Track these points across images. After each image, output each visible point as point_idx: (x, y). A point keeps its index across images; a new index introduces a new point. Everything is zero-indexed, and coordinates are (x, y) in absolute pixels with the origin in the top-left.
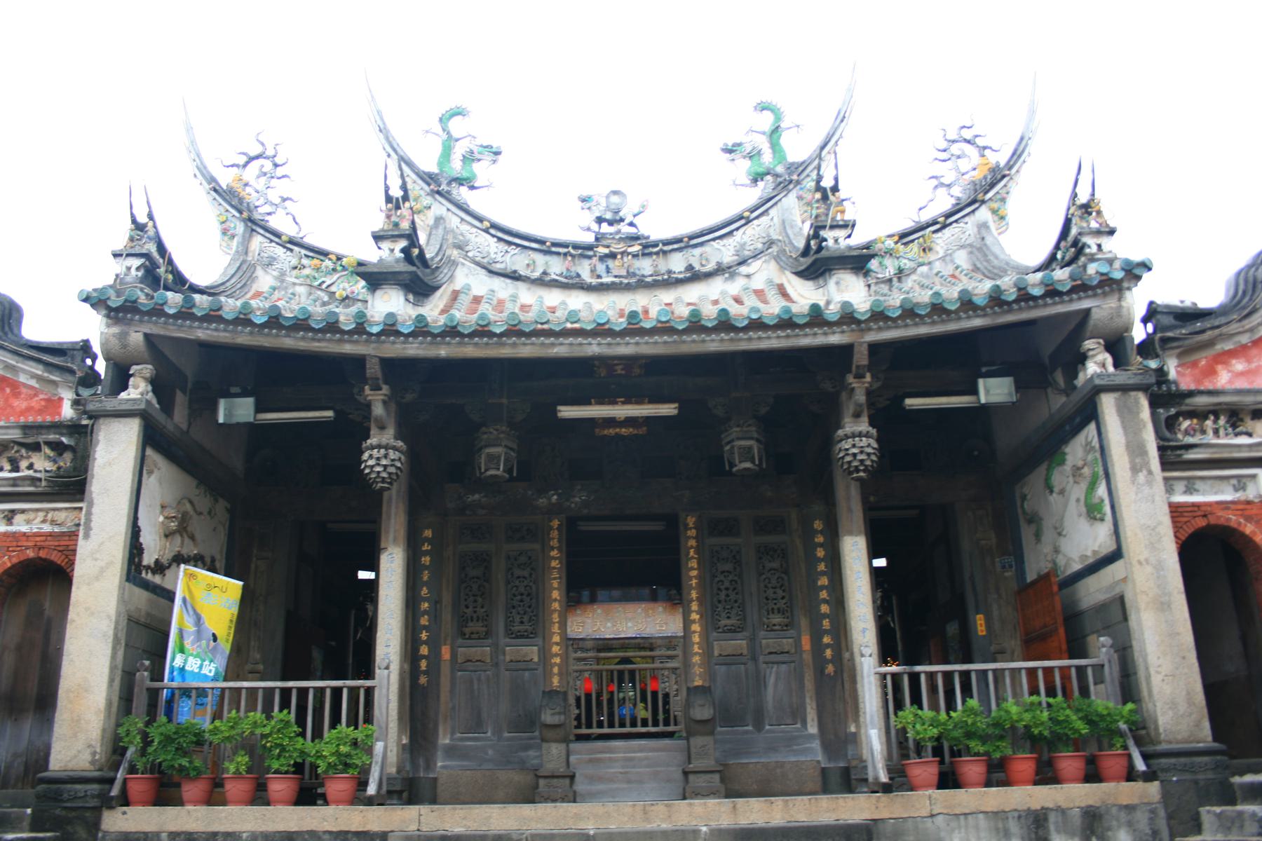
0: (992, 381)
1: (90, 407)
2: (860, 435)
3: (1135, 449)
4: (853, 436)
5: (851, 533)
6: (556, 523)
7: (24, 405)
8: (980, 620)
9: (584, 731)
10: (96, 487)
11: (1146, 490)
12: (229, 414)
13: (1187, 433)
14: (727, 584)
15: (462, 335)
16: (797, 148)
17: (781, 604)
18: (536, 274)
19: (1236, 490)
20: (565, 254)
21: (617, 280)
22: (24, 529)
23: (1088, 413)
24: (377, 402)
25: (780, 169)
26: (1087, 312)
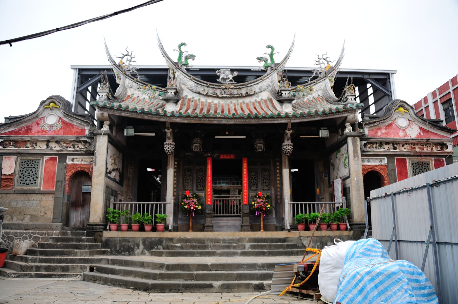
0: (323, 131)
1: (95, 132)
2: (288, 145)
3: (355, 152)
4: (287, 145)
5: (285, 168)
7: (75, 131)
8: (318, 190)
9: (216, 215)
10: (97, 153)
11: (357, 162)
12: (127, 133)
13: (369, 148)
15: (191, 117)
16: (278, 59)
17: (267, 184)
18: (205, 93)
19: (379, 162)
20: (213, 88)
21: (227, 96)
22: (78, 163)
23: (345, 141)
24: (169, 132)
25: (273, 66)
26: (347, 117)
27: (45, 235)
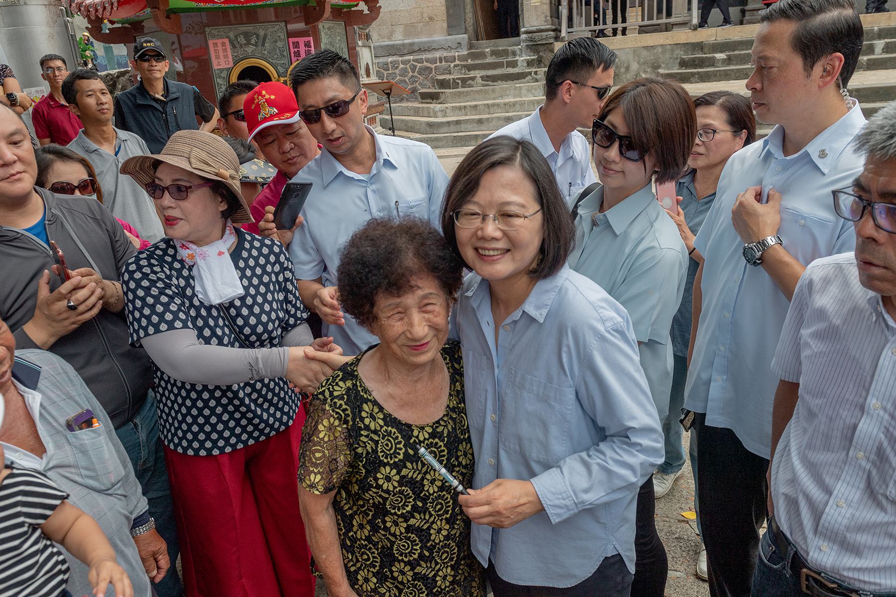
27: (441, 62)
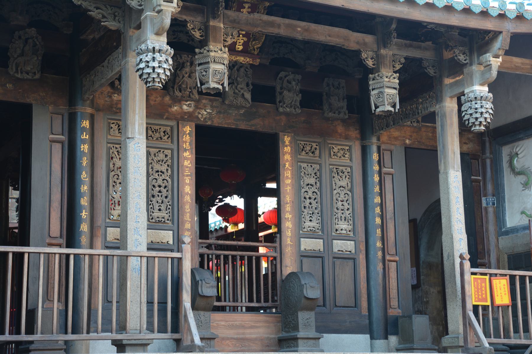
6: (188, 129)
14: (310, 194)
